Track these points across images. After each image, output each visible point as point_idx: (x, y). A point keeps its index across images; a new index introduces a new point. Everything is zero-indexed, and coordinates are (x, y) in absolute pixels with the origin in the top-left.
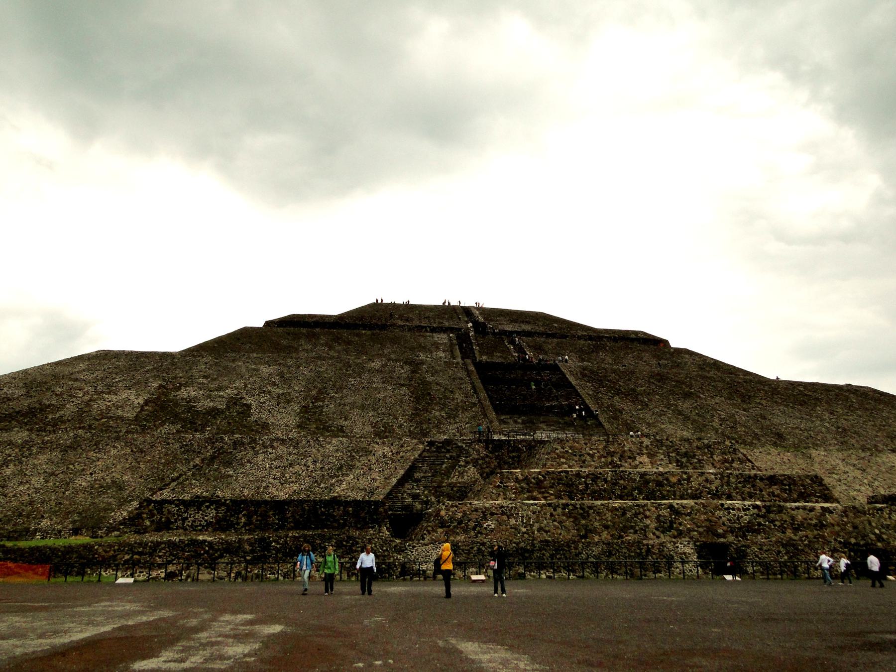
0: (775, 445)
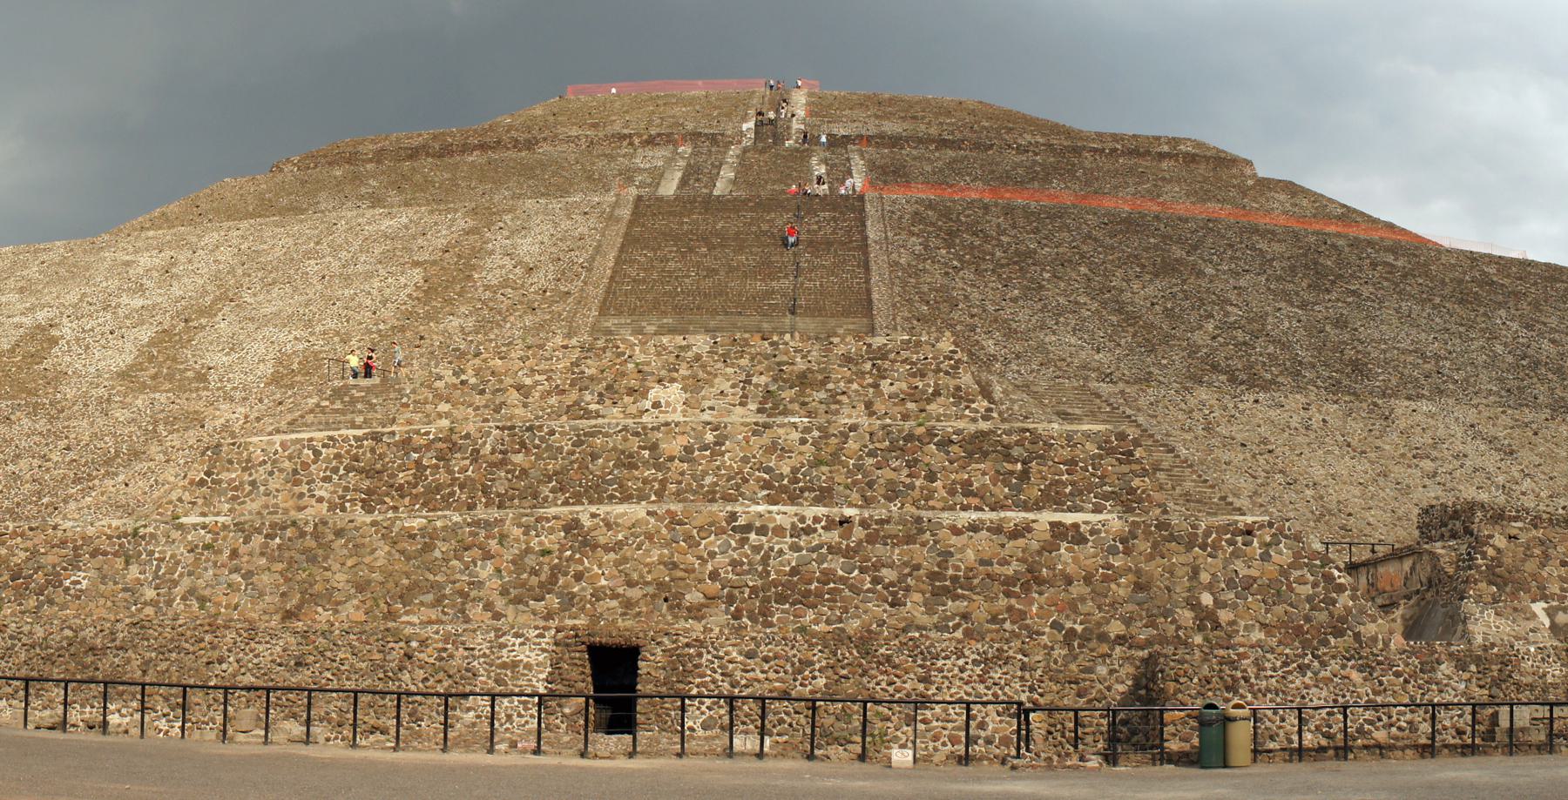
0: (1335, 387)
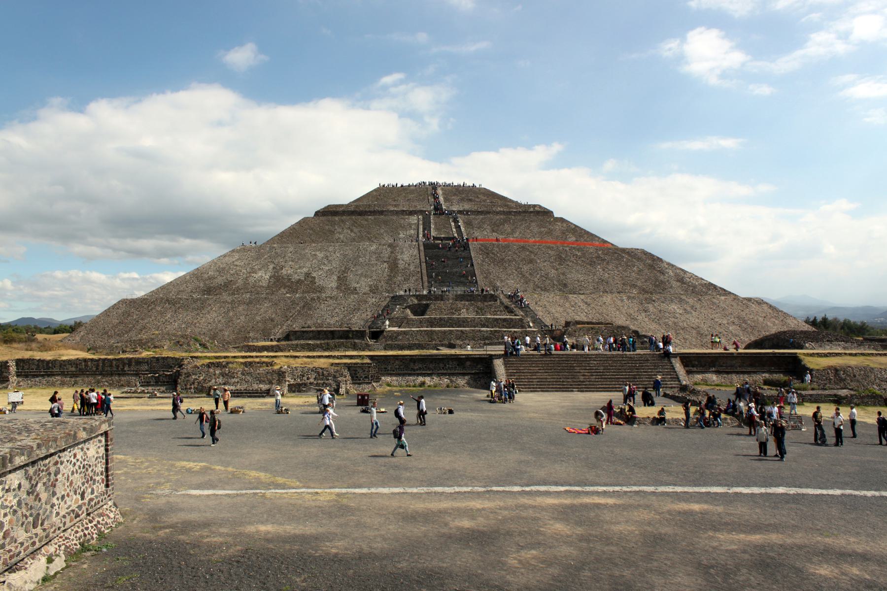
0: (560, 290)
